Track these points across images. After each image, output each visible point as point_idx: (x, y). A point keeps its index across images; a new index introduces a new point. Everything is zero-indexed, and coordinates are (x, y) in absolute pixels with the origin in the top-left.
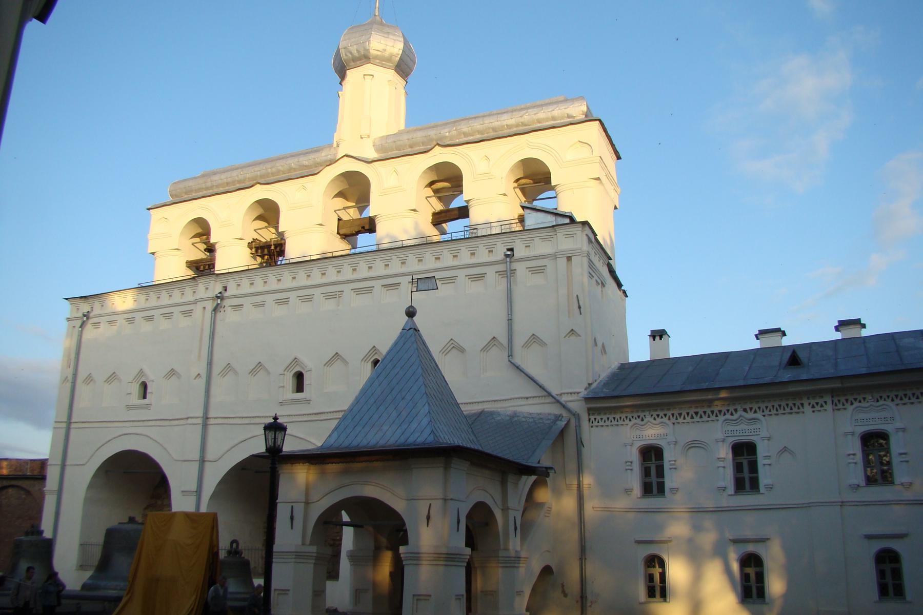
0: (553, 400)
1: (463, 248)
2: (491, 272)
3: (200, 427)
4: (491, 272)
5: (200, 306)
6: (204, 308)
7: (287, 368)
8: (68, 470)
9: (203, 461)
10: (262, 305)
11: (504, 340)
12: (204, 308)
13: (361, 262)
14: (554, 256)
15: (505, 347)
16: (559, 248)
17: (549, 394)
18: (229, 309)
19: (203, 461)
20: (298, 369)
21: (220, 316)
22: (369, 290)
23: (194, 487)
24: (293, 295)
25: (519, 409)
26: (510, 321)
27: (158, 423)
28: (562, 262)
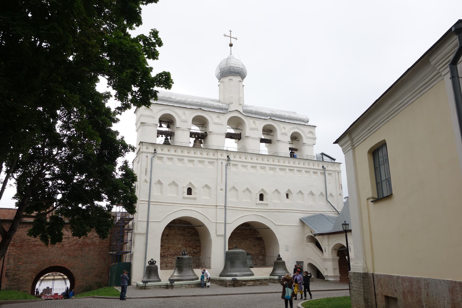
0: (337, 213)
1: (316, 163)
2: (319, 172)
3: (224, 210)
4: (319, 172)
5: (220, 162)
6: (222, 163)
7: (259, 192)
8: (150, 223)
9: (225, 224)
10: (246, 166)
11: (324, 193)
12: (222, 163)
13: (281, 160)
14: (335, 171)
15: (324, 196)
16: (336, 169)
17: (337, 211)
18: (231, 165)
19: (225, 224)
20: (262, 192)
21: (228, 167)
22: (284, 170)
23: (223, 233)
24: (258, 166)
25: (329, 215)
26: (326, 188)
27: (200, 206)
28: (337, 173)
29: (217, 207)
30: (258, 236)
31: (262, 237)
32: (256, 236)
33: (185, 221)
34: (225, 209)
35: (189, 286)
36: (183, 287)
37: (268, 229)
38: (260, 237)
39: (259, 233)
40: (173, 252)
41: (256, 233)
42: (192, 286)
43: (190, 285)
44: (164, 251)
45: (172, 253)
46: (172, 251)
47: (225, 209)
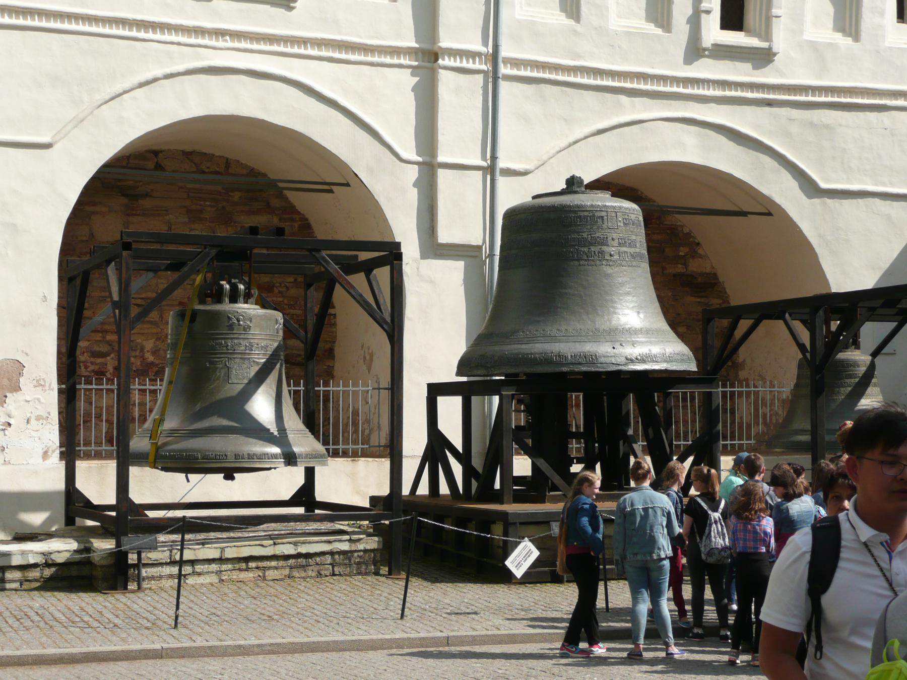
29: (440, 62)
30: (694, 266)
31: (715, 276)
32: (680, 269)
33: (228, 163)
34: (494, 77)
35: (247, 569)
36: (199, 574)
37: (770, 214)
38: (702, 274)
39: (700, 251)
40: (155, 352)
41: (682, 251)
42: (265, 569)
43: (252, 565)
44: (96, 348)
45: (150, 358)
46: (149, 344)
47: (494, 77)
